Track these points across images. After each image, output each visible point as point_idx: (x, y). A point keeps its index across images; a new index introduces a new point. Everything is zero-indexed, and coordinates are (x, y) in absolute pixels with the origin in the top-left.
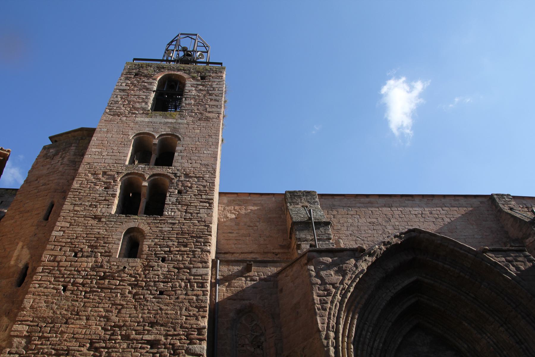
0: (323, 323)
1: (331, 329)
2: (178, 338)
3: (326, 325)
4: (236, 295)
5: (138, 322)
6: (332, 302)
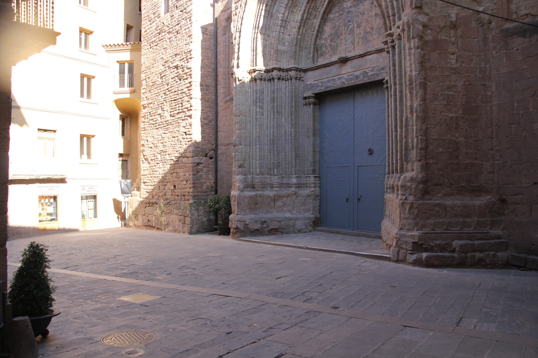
0: (234, 27)
1: (238, 30)
2: (183, 60)
3: (235, 28)
4: (225, 7)
5: (171, 56)
6: (241, 6)
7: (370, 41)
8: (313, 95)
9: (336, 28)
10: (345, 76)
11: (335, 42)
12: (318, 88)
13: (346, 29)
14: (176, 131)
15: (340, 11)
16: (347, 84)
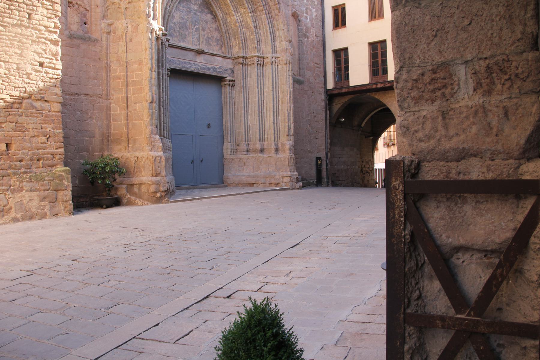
7: (211, 45)
8: (170, 69)
9: (185, 21)
10: (200, 64)
11: (183, 31)
12: (176, 65)
13: (193, 26)
14: (13, 54)
15: (188, 8)
16: (200, 71)
